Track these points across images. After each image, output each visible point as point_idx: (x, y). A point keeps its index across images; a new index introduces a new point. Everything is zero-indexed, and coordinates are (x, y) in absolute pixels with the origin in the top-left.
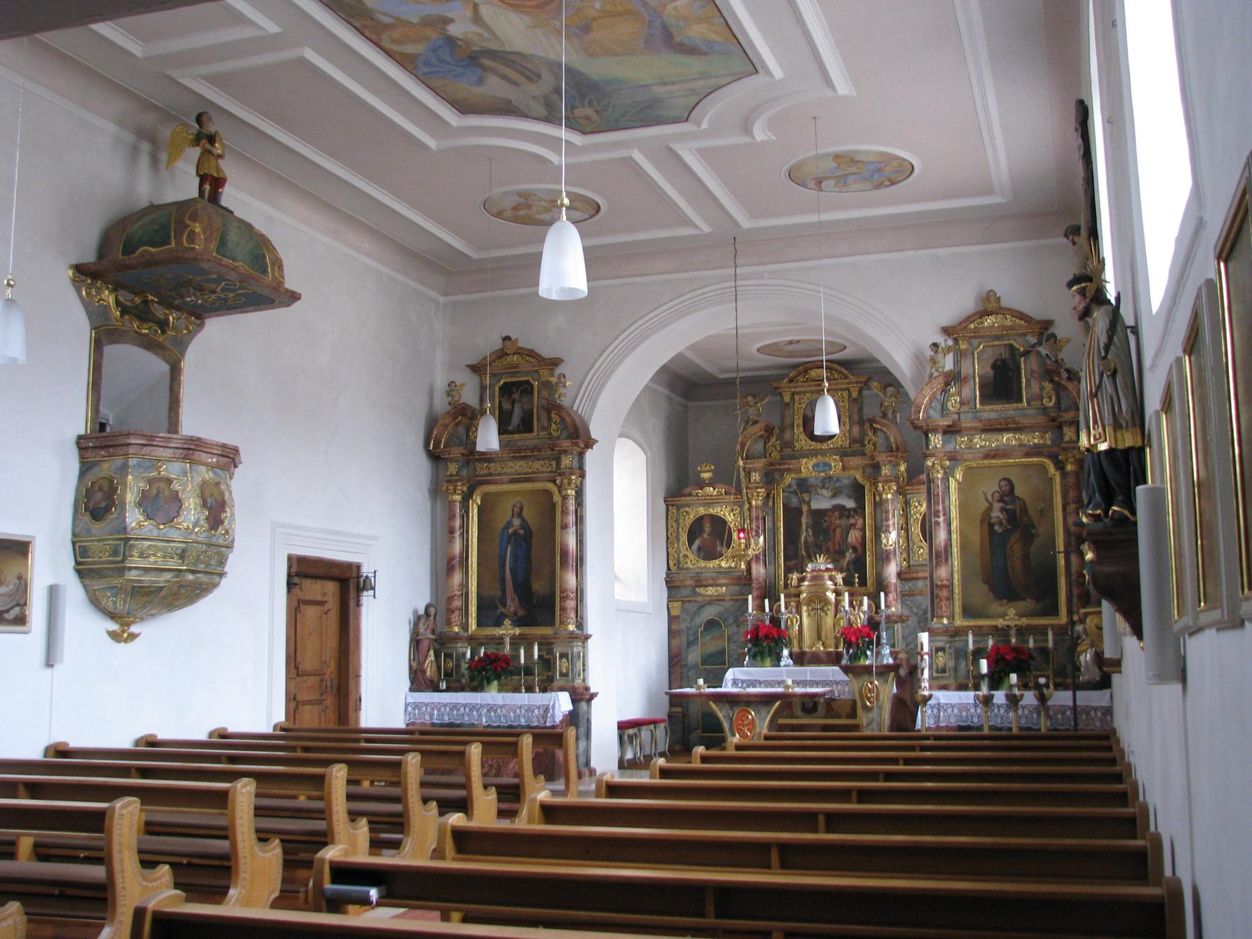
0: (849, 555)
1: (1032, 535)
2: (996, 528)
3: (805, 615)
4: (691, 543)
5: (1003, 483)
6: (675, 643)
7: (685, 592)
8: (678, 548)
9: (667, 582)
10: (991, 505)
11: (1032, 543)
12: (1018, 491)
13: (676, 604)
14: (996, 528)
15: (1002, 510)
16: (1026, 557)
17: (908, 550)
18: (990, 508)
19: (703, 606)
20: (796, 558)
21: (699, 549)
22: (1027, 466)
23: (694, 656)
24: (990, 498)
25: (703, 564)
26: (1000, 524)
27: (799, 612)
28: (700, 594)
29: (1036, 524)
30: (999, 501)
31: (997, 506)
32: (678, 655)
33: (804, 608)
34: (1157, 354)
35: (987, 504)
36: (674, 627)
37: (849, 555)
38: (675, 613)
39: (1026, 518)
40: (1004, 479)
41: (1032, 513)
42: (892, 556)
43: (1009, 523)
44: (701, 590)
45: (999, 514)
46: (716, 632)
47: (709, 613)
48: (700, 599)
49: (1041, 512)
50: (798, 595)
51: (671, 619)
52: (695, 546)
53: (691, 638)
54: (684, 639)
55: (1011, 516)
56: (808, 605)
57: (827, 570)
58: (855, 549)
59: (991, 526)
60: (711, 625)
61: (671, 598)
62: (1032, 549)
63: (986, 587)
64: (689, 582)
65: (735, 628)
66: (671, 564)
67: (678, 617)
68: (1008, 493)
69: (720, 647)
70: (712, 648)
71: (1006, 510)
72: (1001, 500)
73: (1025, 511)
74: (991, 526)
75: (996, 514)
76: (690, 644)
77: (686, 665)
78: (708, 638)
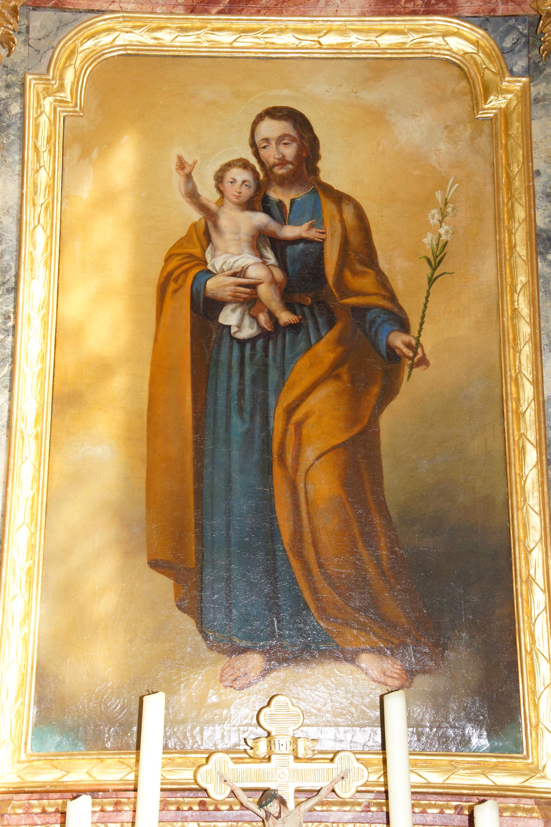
1: (393, 357)
2: (229, 317)
5: (271, 128)
10: (210, 215)
11: (389, 392)
12: (333, 170)
14: (229, 317)
15: (261, 240)
16: (360, 456)
18: (206, 233)
22: (378, 66)
24: (208, 193)
26: (250, 302)
29: (411, 307)
30: (249, 205)
31: (239, 223)
34: (422, 324)
35: (196, 216)
39: (366, 282)
40: (273, 113)
41: (398, 264)
43: (288, 295)
45: (246, 259)
49: (436, 260)
55: (303, 277)
59: (206, 309)
62: (393, 421)
63: (164, 584)
68: (289, 170)
71: (279, 245)
72: (258, 201)
73: (361, 249)
74: (206, 309)
75: (234, 257)
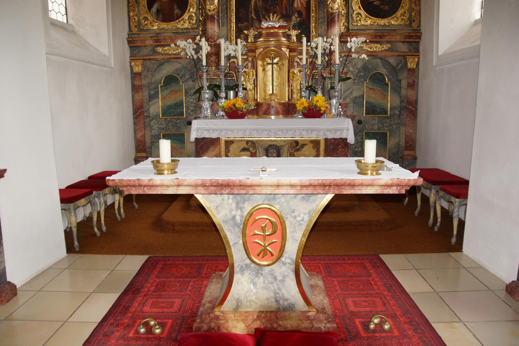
0: (295, 19)
3: (260, 69)
4: (150, 6)
6: (138, 97)
7: (145, 51)
8: (139, 11)
9: (129, 42)
13: (139, 63)
17: (348, 16)
19: (162, 64)
20: (247, 20)
21: (158, 12)
23: (156, 107)
25: (164, 25)
27: (254, 67)
28: (159, 53)
32: (141, 107)
33: (260, 63)
36: (137, 83)
37: (295, 19)
38: (138, 69)
42: (336, 18)
44: (160, 49)
46: (174, 87)
47: (168, 70)
48: (159, 57)
50: (254, 51)
51: (135, 76)
52: (154, 9)
53: (153, 92)
54: (146, 93)
56: (263, 60)
57: (280, 27)
58: (300, 14)
60: (170, 80)
61: (133, 57)
64: (149, 42)
65: (190, 83)
66: (133, 26)
67: (140, 74)
69: (178, 99)
70: (171, 101)
76: (153, 97)
77: (148, 116)
78: (166, 92)
